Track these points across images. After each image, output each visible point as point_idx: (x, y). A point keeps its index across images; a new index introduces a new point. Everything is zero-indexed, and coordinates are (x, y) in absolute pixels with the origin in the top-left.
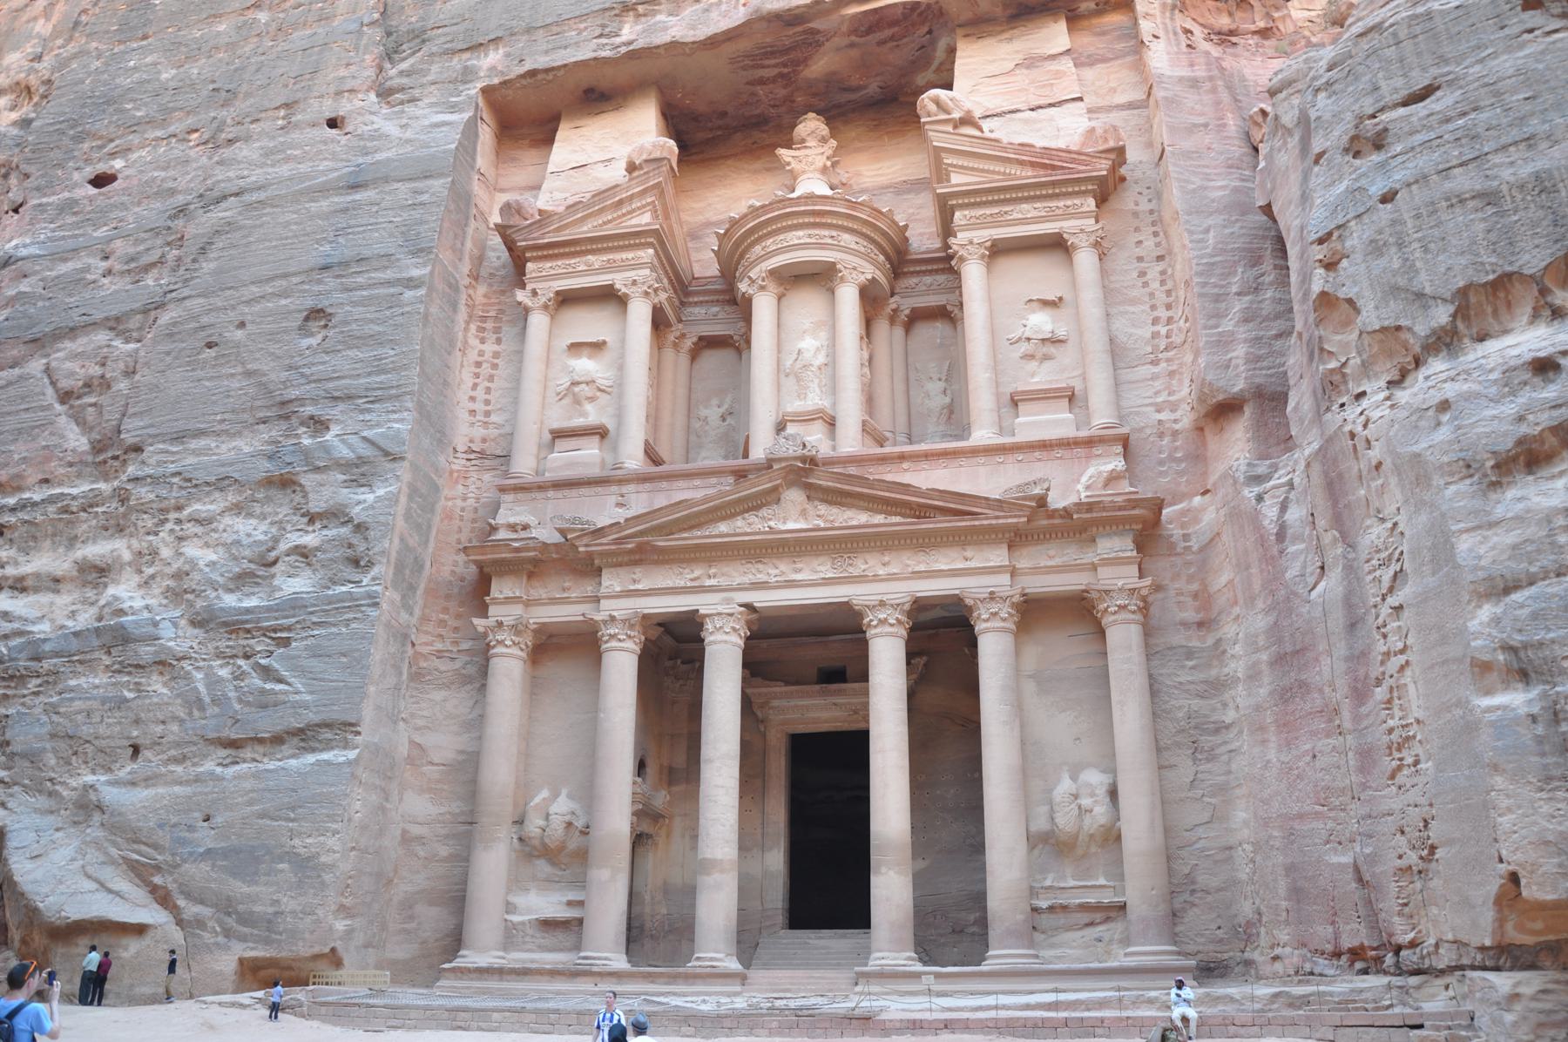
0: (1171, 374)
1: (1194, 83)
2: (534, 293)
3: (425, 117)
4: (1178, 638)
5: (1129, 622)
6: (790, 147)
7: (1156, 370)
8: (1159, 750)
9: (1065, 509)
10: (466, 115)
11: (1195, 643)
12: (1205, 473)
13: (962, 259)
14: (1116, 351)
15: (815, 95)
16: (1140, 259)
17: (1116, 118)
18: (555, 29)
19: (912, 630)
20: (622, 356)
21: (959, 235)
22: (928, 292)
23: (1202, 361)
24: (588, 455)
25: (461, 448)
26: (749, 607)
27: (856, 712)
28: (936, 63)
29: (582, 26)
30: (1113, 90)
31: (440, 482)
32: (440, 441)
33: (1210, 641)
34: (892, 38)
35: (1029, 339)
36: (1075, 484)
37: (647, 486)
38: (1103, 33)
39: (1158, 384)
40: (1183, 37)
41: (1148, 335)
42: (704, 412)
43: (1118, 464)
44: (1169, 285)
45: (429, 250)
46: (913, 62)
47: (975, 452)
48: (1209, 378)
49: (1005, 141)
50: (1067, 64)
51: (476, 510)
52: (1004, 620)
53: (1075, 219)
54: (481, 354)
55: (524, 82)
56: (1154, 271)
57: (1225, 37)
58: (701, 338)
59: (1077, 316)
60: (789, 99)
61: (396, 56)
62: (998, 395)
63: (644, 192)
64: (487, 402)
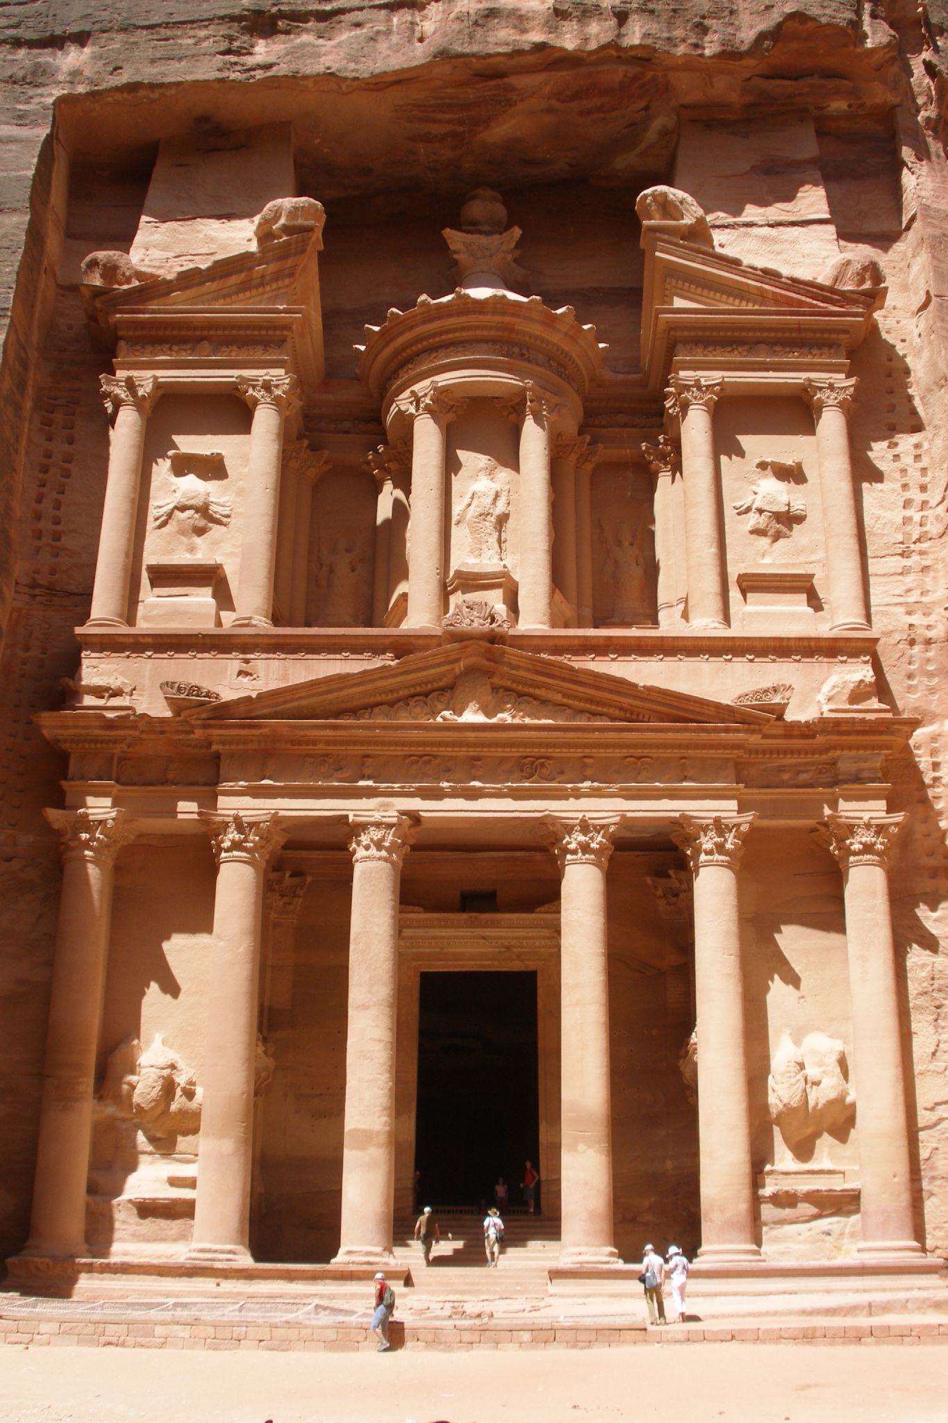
0: (925, 569)
10: (43, 132)
18: (164, 32)
19: (611, 859)
26: (414, 818)
27: (508, 948)
28: (643, 145)
35: (760, 511)
36: (817, 693)
39: (909, 580)
41: (899, 520)
43: (867, 674)
44: (925, 462)
49: (745, 262)
55: (119, 97)
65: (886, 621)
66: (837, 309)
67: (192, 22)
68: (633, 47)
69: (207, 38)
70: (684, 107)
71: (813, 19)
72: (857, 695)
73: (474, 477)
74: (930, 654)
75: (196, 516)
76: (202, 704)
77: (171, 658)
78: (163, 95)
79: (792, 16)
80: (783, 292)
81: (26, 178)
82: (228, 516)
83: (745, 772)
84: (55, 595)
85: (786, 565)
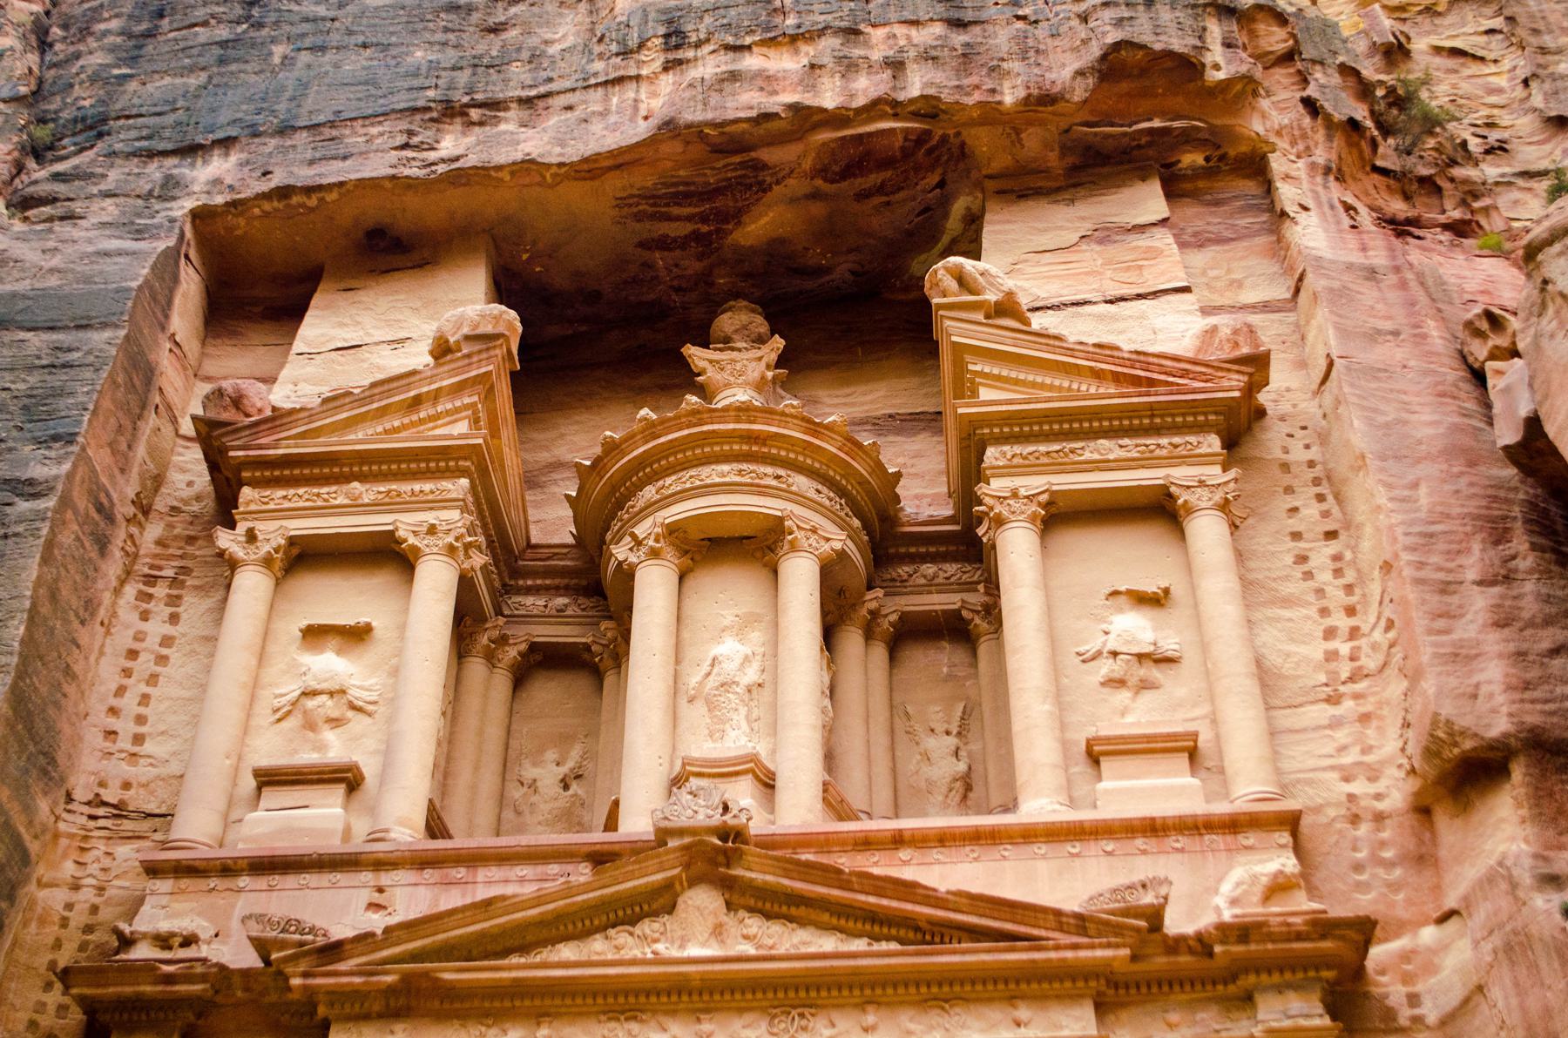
0: (1365, 718)
1: (1372, 274)
2: (251, 537)
3: (90, 241)
6: (706, 345)
9: (1199, 937)
12: (1437, 890)
14: (1266, 677)
15: (747, 275)
16: (1296, 536)
18: (328, 132)
20: (399, 653)
22: (931, 586)
23: (1429, 685)
24: (320, 818)
25: (80, 794)
29: (374, 130)
30: (1239, 284)
31: (33, 847)
32: (44, 772)
34: (881, 189)
35: (1115, 654)
36: (1209, 894)
37: (428, 873)
38: (1217, 203)
39: (1342, 736)
40: (1343, 215)
41: (1320, 656)
42: (529, 772)
44: (1350, 576)
45: (70, 439)
46: (910, 234)
47: (1029, 835)
48: (1447, 710)
49: (1072, 339)
50: (1164, 240)
51: (94, 909)
54: (139, 637)
55: (267, 206)
56: (1321, 555)
57: (1401, 228)
58: (534, 647)
60: (705, 279)
61: (49, 155)
62: (1065, 745)
63: (459, 388)
64: (141, 720)
65: (1310, 791)
67: (364, 118)
68: (912, 101)
69: (382, 134)
70: (990, 177)
71: (1142, 47)
73: (718, 638)
74: (1385, 835)
75: (330, 703)
76: (301, 944)
77: (271, 889)
78: (322, 200)
79: (1117, 46)
80: (1125, 370)
81: (129, 289)
82: (375, 703)
83: (1112, 1017)
84: (126, 817)
85: (1154, 723)
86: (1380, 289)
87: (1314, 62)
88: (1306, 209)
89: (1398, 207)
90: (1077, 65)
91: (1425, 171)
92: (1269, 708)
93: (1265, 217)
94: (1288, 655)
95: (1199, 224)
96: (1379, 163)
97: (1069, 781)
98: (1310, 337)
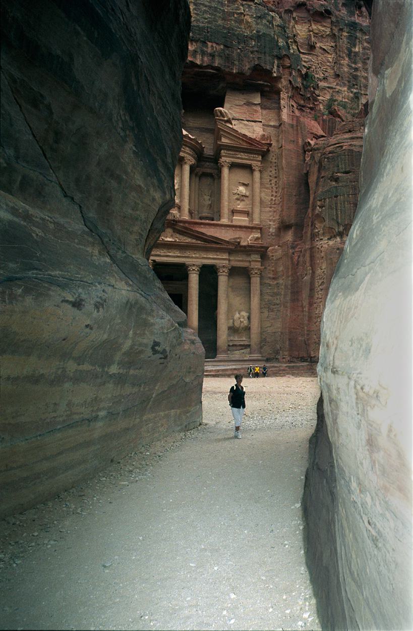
0: (275, 212)
1: (292, 126)
4: (267, 282)
5: (257, 277)
7: (271, 210)
8: (261, 308)
11: (271, 283)
13: (223, 166)
14: (261, 202)
16: (270, 176)
17: (269, 130)
21: (222, 158)
33: (275, 283)
35: (238, 194)
36: (248, 239)
38: (270, 99)
47: (222, 226)
49: (239, 132)
50: (259, 108)
52: (226, 273)
53: (256, 163)
57: (301, 108)
59: (253, 190)
66: (260, 147)
72: (257, 239)
86: (293, 130)
87: (293, 69)
88: (284, 107)
89: (302, 102)
90: (249, 67)
91: (309, 96)
92: (261, 207)
93: (277, 105)
94: (265, 198)
95: (265, 104)
96: (301, 93)
97: (229, 216)
98: (280, 137)
